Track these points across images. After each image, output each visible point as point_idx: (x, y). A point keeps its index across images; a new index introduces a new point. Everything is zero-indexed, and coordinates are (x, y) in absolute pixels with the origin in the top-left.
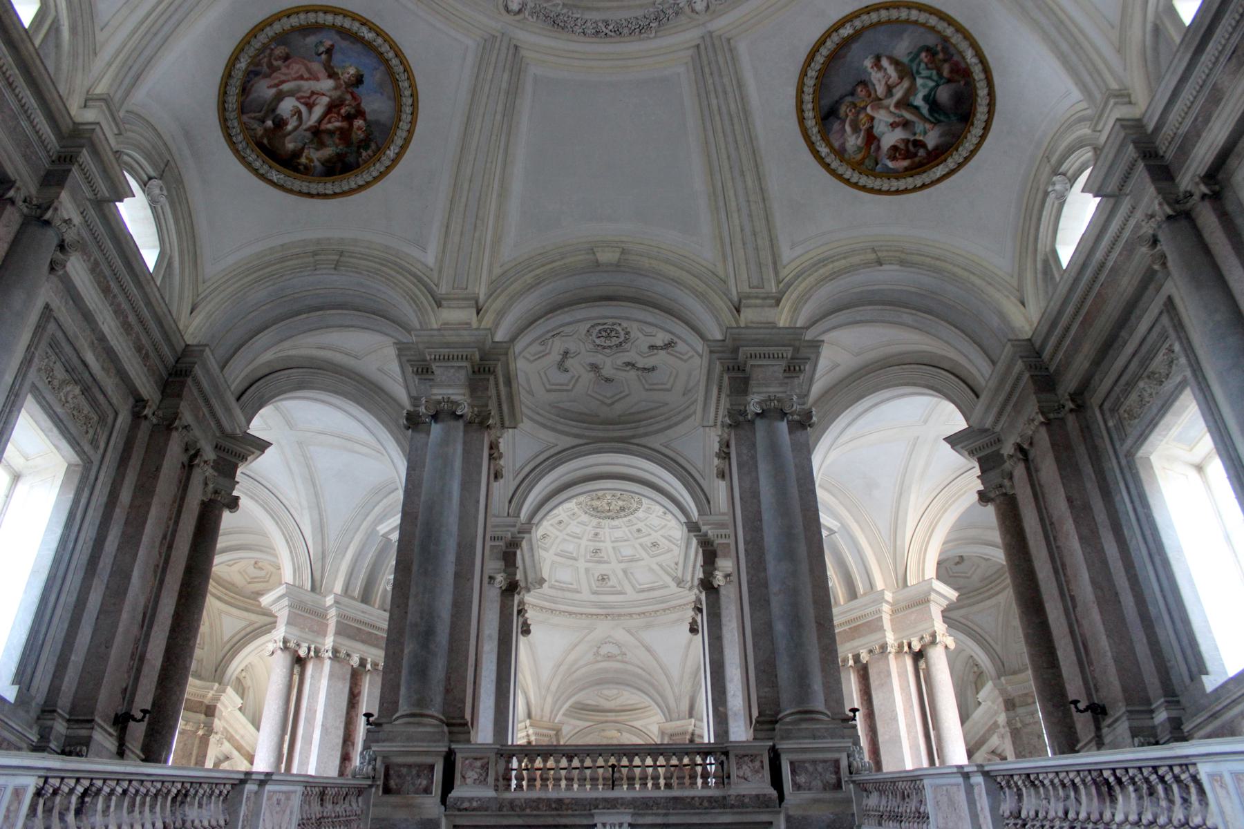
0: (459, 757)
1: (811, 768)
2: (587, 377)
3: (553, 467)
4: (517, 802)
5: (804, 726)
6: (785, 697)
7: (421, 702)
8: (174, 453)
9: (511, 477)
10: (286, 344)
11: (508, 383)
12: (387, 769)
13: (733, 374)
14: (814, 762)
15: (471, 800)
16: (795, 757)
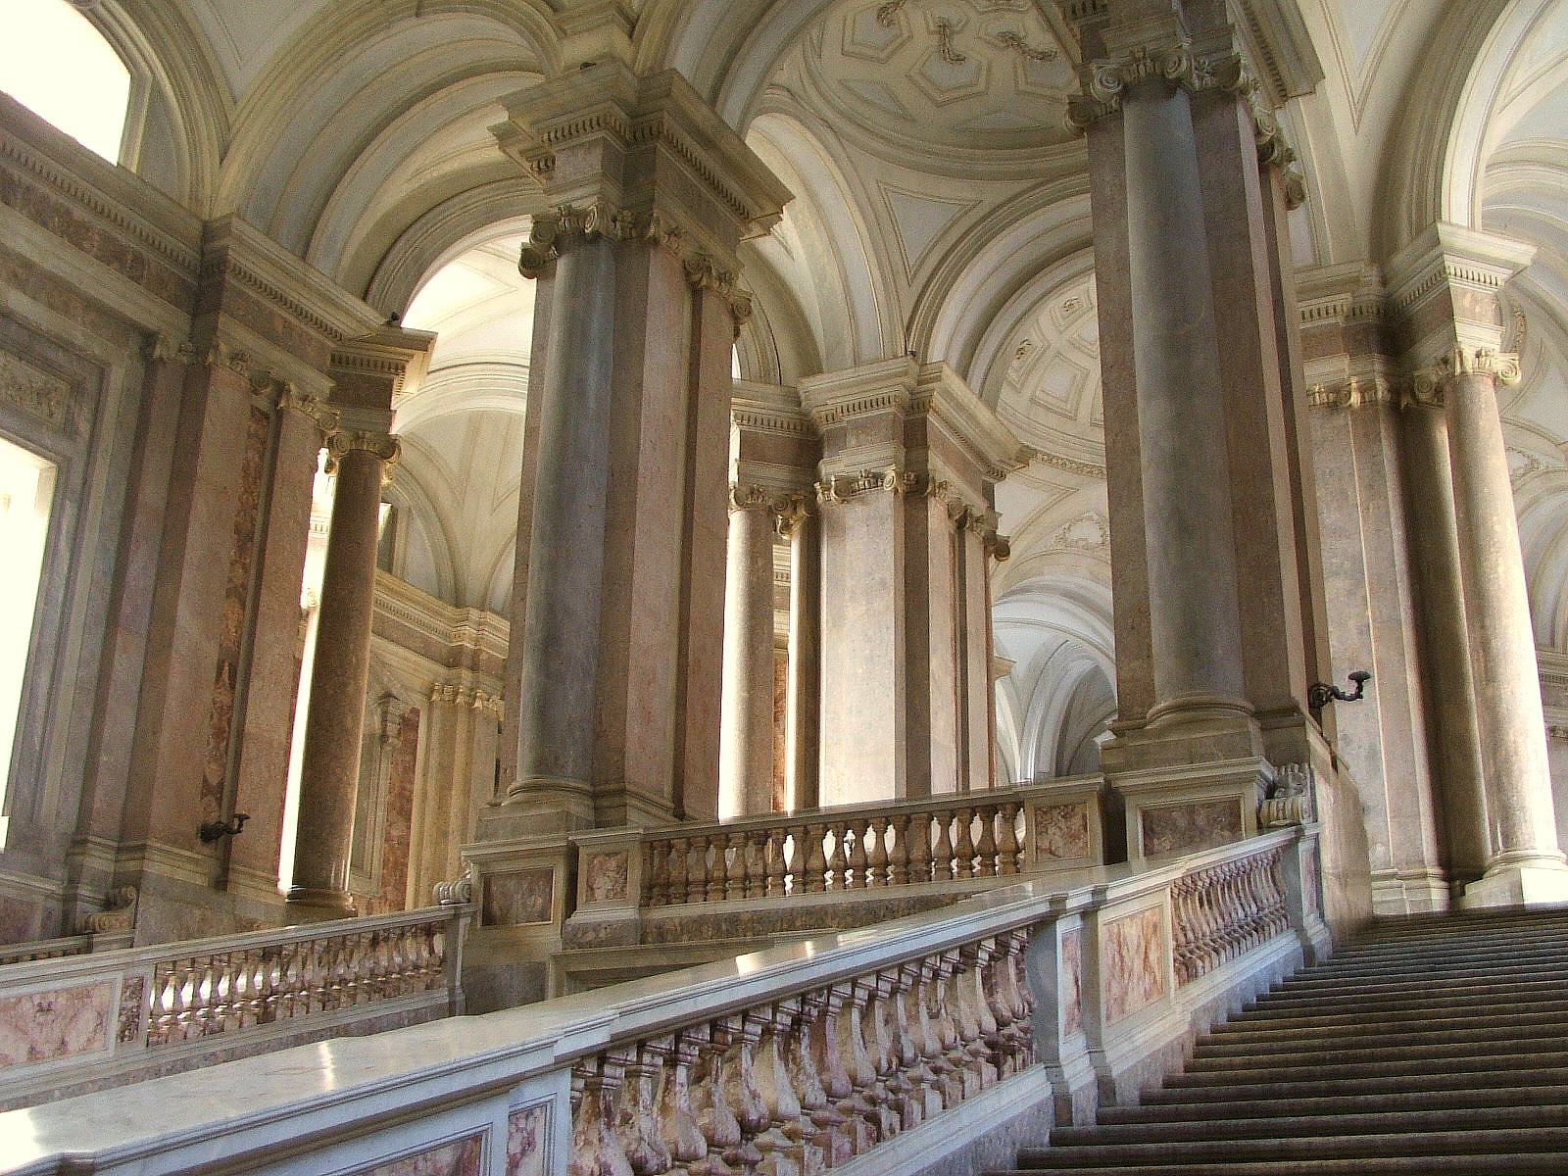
0: (583, 853)
1: (1182, 823)
2: (1005, 62)
3: (980, 246)
4: (669, 925)
5: (1174, 737)
6: (1158, 677)
7: (543, 764)
8: (227, 400)
9: (902, 281)
10: (417, 161)
11: (708, 143)
12: (487, 880)
13: (1083, 21)
14: (1191, 810)
15: (596, 927)
16: (1151, 802)
